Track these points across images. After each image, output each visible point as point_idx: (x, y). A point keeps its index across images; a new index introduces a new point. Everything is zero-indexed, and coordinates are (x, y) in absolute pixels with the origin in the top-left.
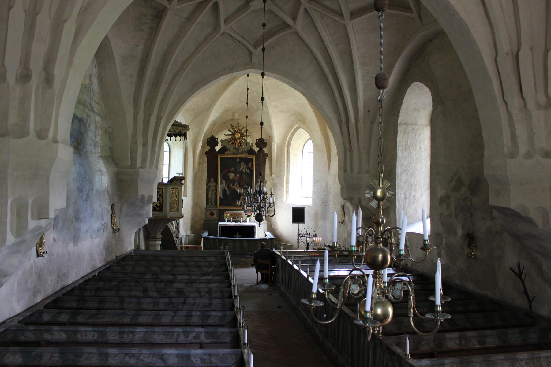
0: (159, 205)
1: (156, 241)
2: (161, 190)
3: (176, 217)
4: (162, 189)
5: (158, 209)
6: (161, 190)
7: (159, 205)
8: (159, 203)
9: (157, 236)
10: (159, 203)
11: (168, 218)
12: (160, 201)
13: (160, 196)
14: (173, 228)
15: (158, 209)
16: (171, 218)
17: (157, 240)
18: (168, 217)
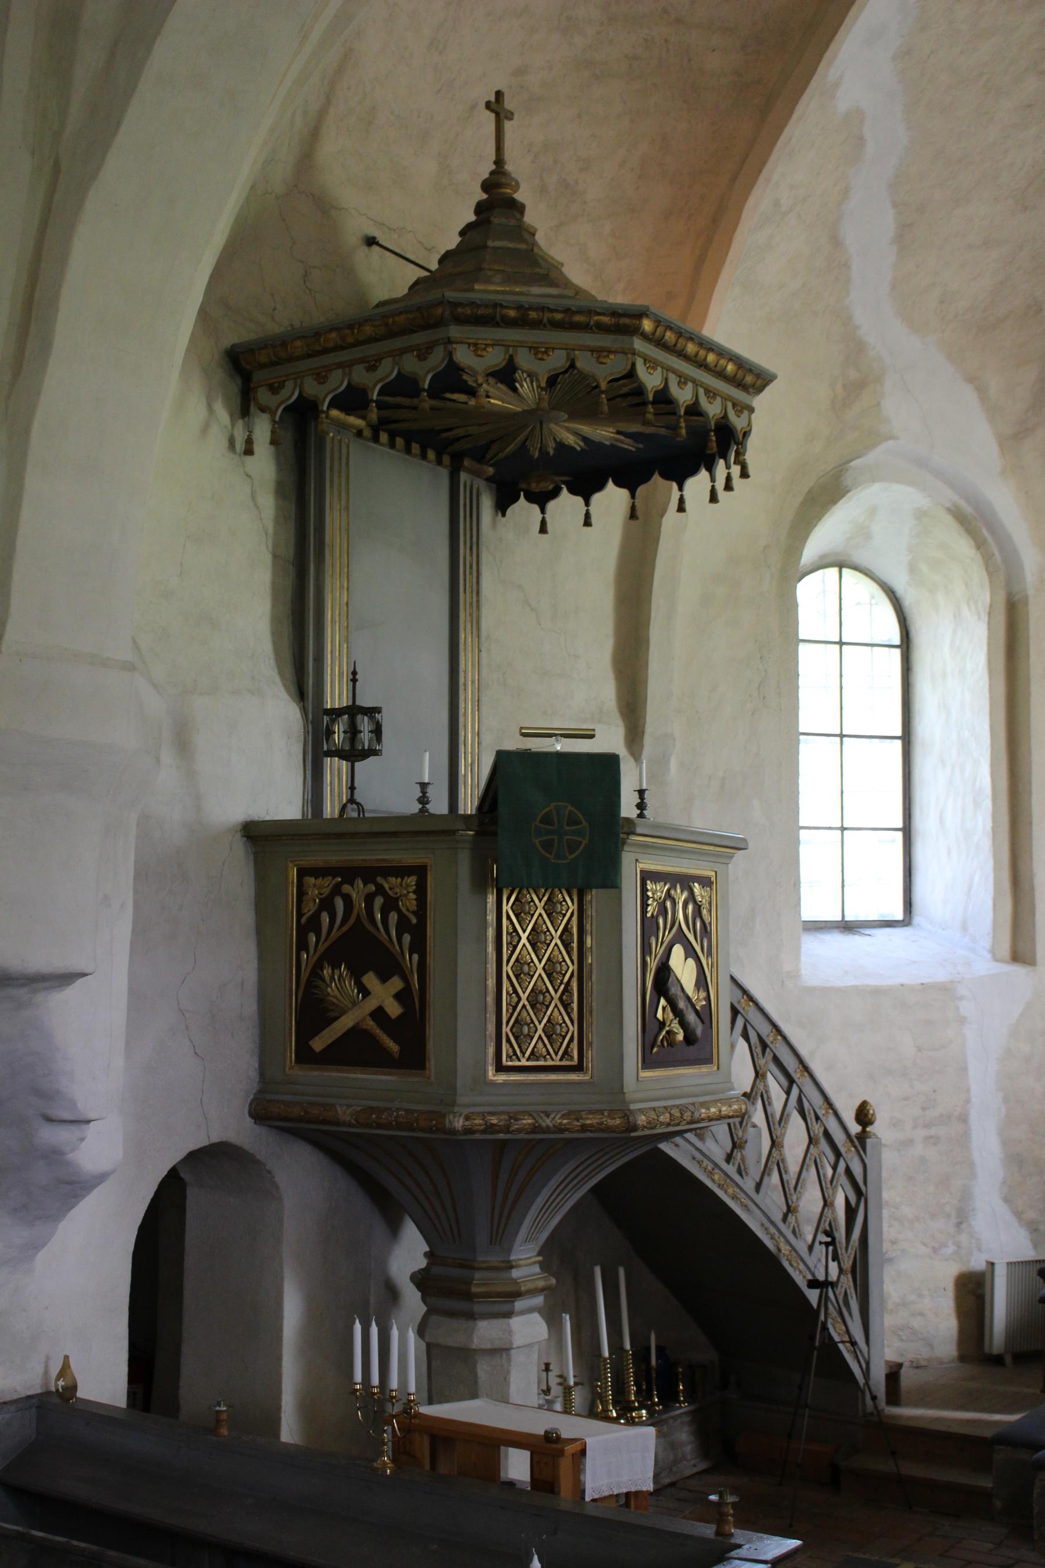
0: (394, 1010)
1: (471, 1316)
2: (412, 880)
3: (547, 1122)
4: (420, 872)
5: (393, 1047)
6: (412, 880)
7: (394, 1010)
8: (398, 997)
9: (478, 1275)
10: (398, 997)
11: (453, 1132)
12: (405, 979)
13: (407, 938)
14: (790, 1210)
15: (393, 1047)
16: (490, 1128)
17: (478, 1308)
18: (459, 1123)
